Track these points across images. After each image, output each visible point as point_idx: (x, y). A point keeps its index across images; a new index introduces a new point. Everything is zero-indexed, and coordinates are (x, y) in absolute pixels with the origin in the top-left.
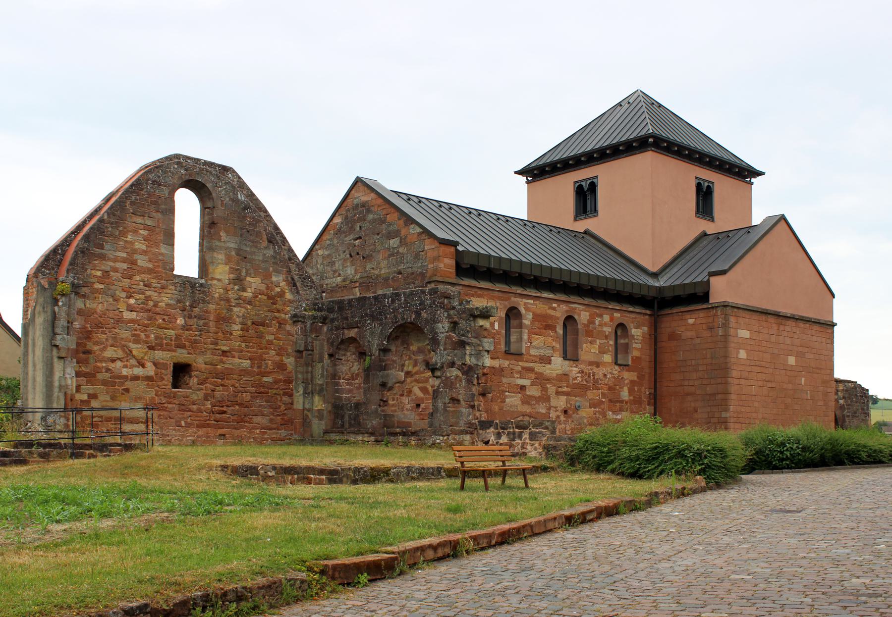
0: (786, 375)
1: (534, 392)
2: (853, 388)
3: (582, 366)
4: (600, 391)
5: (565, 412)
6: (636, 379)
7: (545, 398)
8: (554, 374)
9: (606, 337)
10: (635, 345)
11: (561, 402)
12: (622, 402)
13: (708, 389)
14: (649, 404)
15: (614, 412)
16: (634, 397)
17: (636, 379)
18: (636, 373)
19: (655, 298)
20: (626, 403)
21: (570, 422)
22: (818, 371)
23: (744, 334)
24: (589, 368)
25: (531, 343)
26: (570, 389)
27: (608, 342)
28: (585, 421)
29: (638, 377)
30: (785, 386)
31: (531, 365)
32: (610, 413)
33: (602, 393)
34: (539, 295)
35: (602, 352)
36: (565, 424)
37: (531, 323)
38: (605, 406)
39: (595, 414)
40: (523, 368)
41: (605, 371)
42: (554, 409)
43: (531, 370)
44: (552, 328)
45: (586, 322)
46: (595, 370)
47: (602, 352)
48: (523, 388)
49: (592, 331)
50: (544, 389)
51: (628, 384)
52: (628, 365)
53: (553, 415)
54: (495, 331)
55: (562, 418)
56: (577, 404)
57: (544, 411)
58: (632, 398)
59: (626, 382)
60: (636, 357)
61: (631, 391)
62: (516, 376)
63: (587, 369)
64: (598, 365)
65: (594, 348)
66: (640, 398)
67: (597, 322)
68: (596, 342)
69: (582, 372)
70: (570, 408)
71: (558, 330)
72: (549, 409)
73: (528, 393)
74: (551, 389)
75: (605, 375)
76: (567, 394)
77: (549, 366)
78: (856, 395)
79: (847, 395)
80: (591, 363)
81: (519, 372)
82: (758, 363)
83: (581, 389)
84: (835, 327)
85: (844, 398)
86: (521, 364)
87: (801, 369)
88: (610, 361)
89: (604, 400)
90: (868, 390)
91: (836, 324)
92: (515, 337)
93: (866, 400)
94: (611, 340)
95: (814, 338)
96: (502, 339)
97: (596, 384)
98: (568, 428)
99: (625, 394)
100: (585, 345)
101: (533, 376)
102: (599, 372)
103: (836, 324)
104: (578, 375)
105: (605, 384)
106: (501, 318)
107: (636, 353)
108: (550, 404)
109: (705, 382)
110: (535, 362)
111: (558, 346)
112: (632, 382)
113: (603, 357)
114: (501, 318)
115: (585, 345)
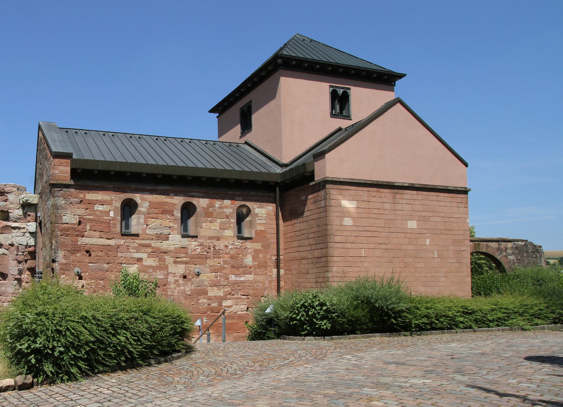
0: (405, 237)
1: (150, 262)
2: (523, 245)
3: (202, 241)
4: (222, 259)
5: (185, 277)
6: (260, 248)
7: (163, 267)
8: (172, 248)
9: (227, 217)
10: (258, 221)
11: (181, 269)
12: (246, 267)
13: (316, 253)
14: (274, 268)
15: (236, 275)
16: (258, 263)
17: (260, 248)
18: (260, 244)
19: (276, 183)
20: (250, 267)
21: (189, 284)
22: (447, 232)
23: (347, 204)
24: (209, 241)
25: (147, 225)
26: (189, 259)
27: (230, 220)
28: (206, 283)
29: (262, 247)
30: (404, 247)
31: (148, 242)
32: (233, 276)
33: (223, 261)
34: (154, 188)
35: (223, 228)
36: (183, 286)
37: (148, 210)
38: (227, 271)
39: (217, 277)
40: (140, 245)
41: (226, 243)
42: (173, 275)
43: (149, 246)
44: (171, 213)
45: (205, 206)
46: (216, 243)
47: (223, 228)
48: (139, 260)
49: (212, 213)
50: (162, 260)
51: (251, 253)
52: (251, 238)
53: (171, 279)
54: (110, 218)
55: (181, 281)
56: (196, 271)
57: (162, 277)
58: (256, 263)
59: (250, 251)
60: (260, 231)
61: (254, 258)
62: (131, 251)
63: (207, 243)
64: (218, 239)
65: (214, 225)
66: (266, 262)
67: (217, 206)
68: (216, 221)
69: (201, 245)
70: (189, 274)
71: (175, 213)
72: (168, 275)
73: (145, 263)
74: (169, 259)
75: (226, 246)
76: (186, 263)
77: (167, 242)
78: (527, 251)
79: (516, 252)
80: (211, 238)
81: (135, 248)
82: (367, 229)
83: (201, 258)
84: (469, 192)
85: (513, 254)
86: (136, 241)
87: (425, 231)
88: (232, 234)
89: (225, 266)
90: (540, 247)
91: (470, 190)
92: (135, 221)
93: (538, 255)
94: (232, 218)
95: (443, 204)
96: (117, 223)
97: (217, 254)
98: (187, 289)
99: (249, 260)
100: (204, 224)
101: (150, 250)
102: (220, 245)
103: (470, 190)
104: (197, 247)
105: (227, 253)
106: (116, 208)
107: (260, 228)
108: (167, 272)
109: (313, 248)
110: (152, 239)
111: (177, 225)
112: (255, 250)
113: (224, 232)
114: (116, 208)
115: (204, 224)
